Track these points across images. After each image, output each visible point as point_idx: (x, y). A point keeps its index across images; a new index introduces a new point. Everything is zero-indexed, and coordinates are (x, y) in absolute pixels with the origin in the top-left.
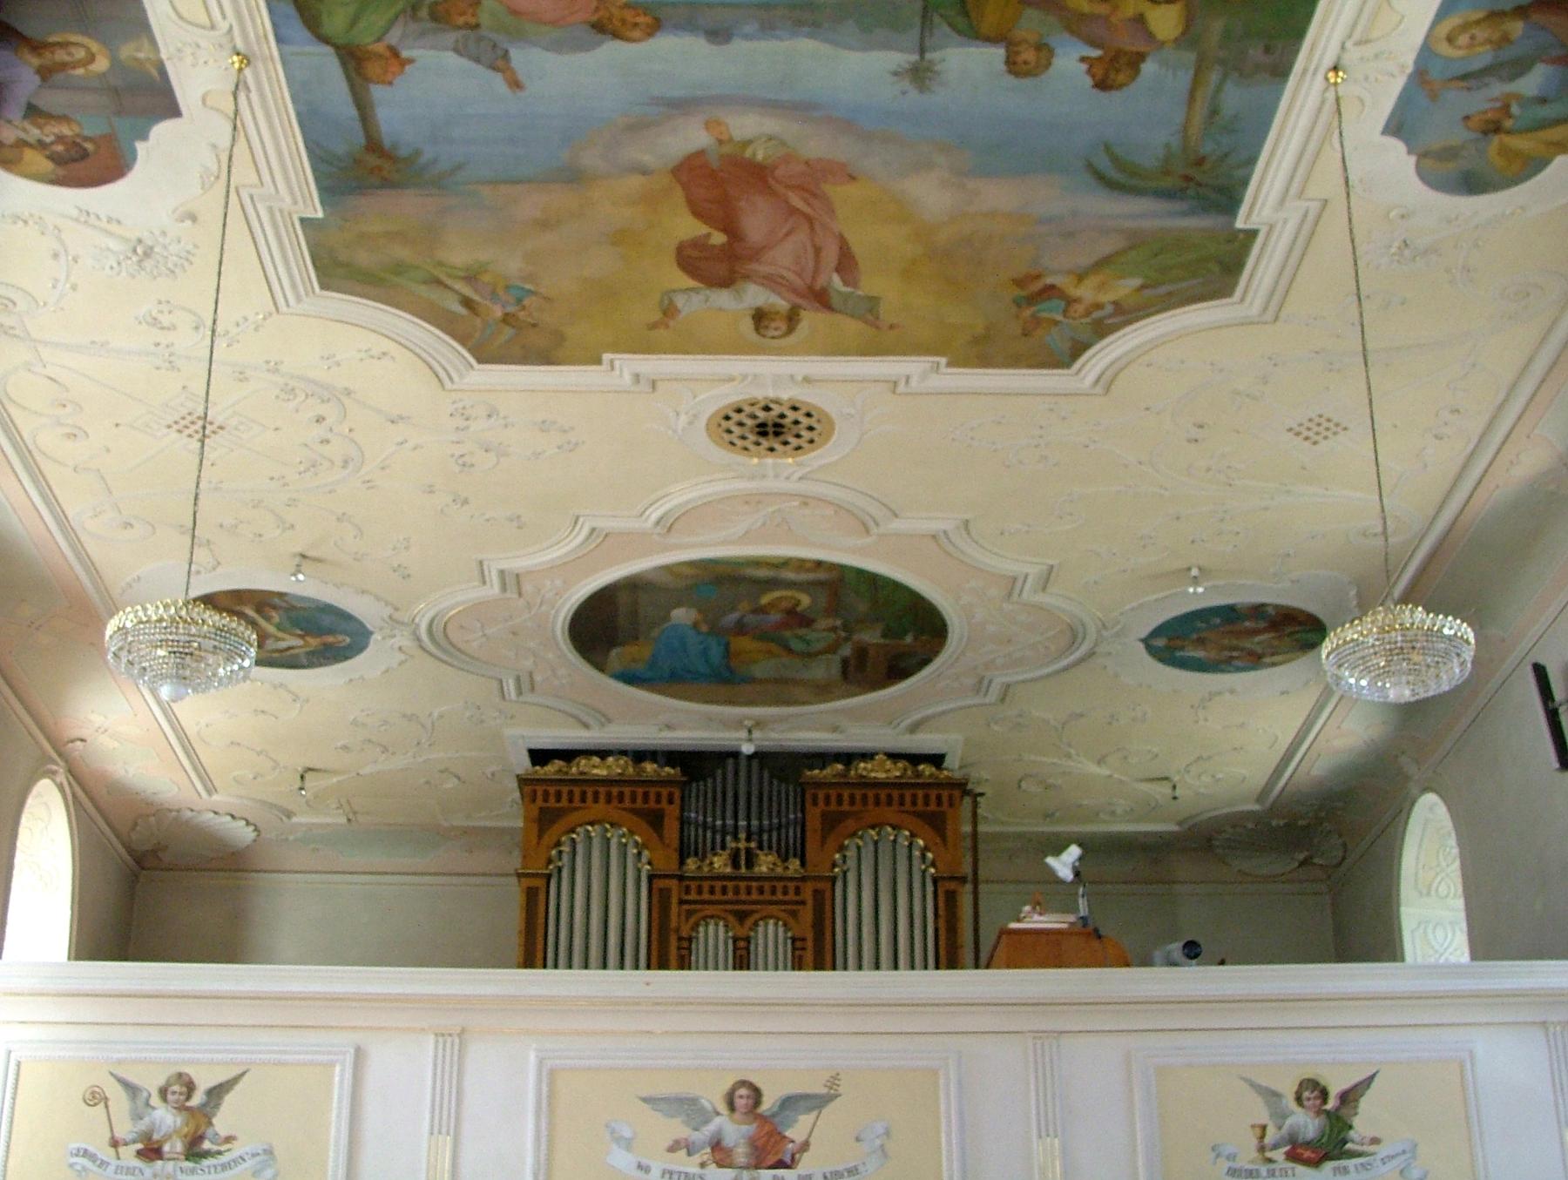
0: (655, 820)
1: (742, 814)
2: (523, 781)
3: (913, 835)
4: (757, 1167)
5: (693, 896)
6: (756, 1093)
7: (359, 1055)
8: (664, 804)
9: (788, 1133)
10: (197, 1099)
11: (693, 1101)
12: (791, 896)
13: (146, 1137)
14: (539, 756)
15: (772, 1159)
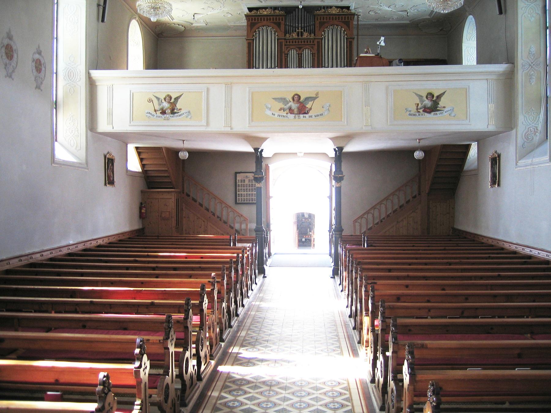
0: (279, 25)
1: (300, 22)
4: (299, 114)
5: (288, 43)
7: (208, 90)
8: (281, 21)
9: (307, 106)
10: (172, 100)
11: (285, 99)
13: (162, 109)
14: (250, 9)
15: (303, 112)
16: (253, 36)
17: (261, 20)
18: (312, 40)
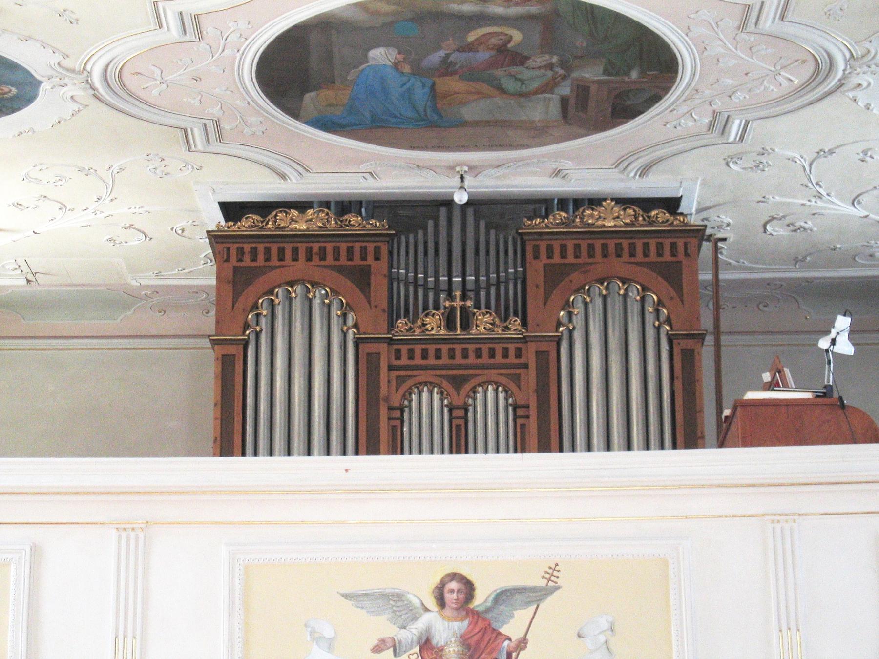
2: (215, 238)
3: (644, 289)
5: (404, 361)
6: (469, 587)
7: (36, 552)
8: (370, 260)
9: (505, 630)
11: (399, 597)
12: (512, 359)
14: (233, 211)
16: (246, 326)
17: (281, 259)
18: (512, 347)
